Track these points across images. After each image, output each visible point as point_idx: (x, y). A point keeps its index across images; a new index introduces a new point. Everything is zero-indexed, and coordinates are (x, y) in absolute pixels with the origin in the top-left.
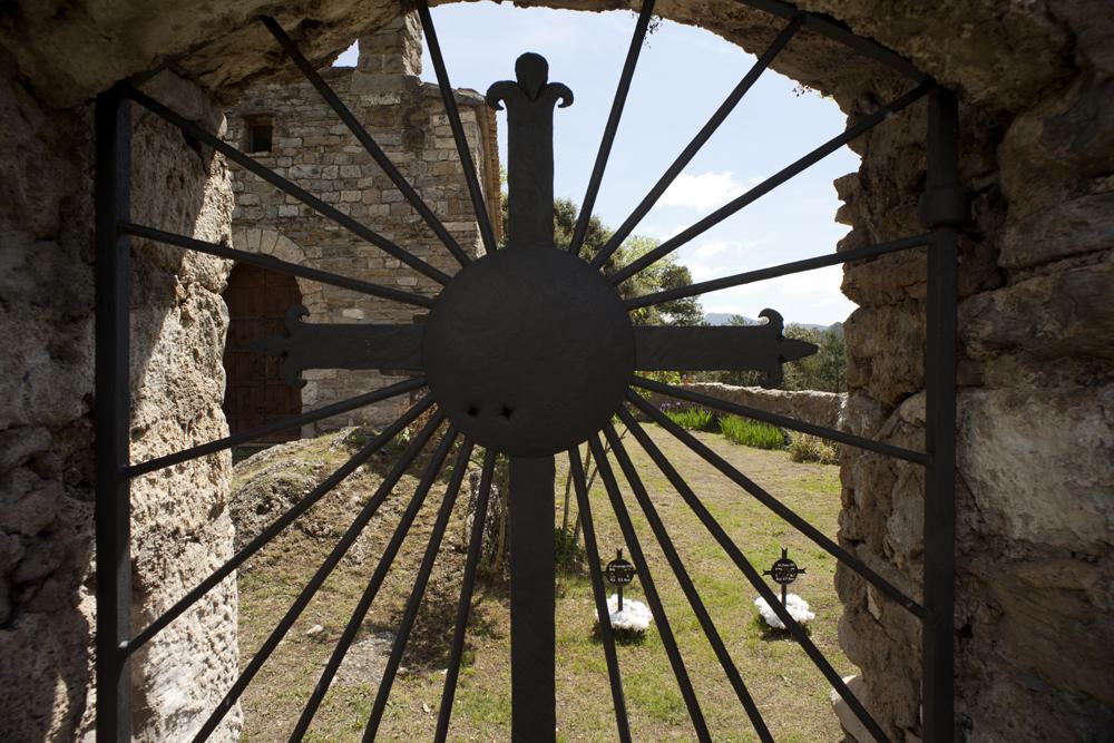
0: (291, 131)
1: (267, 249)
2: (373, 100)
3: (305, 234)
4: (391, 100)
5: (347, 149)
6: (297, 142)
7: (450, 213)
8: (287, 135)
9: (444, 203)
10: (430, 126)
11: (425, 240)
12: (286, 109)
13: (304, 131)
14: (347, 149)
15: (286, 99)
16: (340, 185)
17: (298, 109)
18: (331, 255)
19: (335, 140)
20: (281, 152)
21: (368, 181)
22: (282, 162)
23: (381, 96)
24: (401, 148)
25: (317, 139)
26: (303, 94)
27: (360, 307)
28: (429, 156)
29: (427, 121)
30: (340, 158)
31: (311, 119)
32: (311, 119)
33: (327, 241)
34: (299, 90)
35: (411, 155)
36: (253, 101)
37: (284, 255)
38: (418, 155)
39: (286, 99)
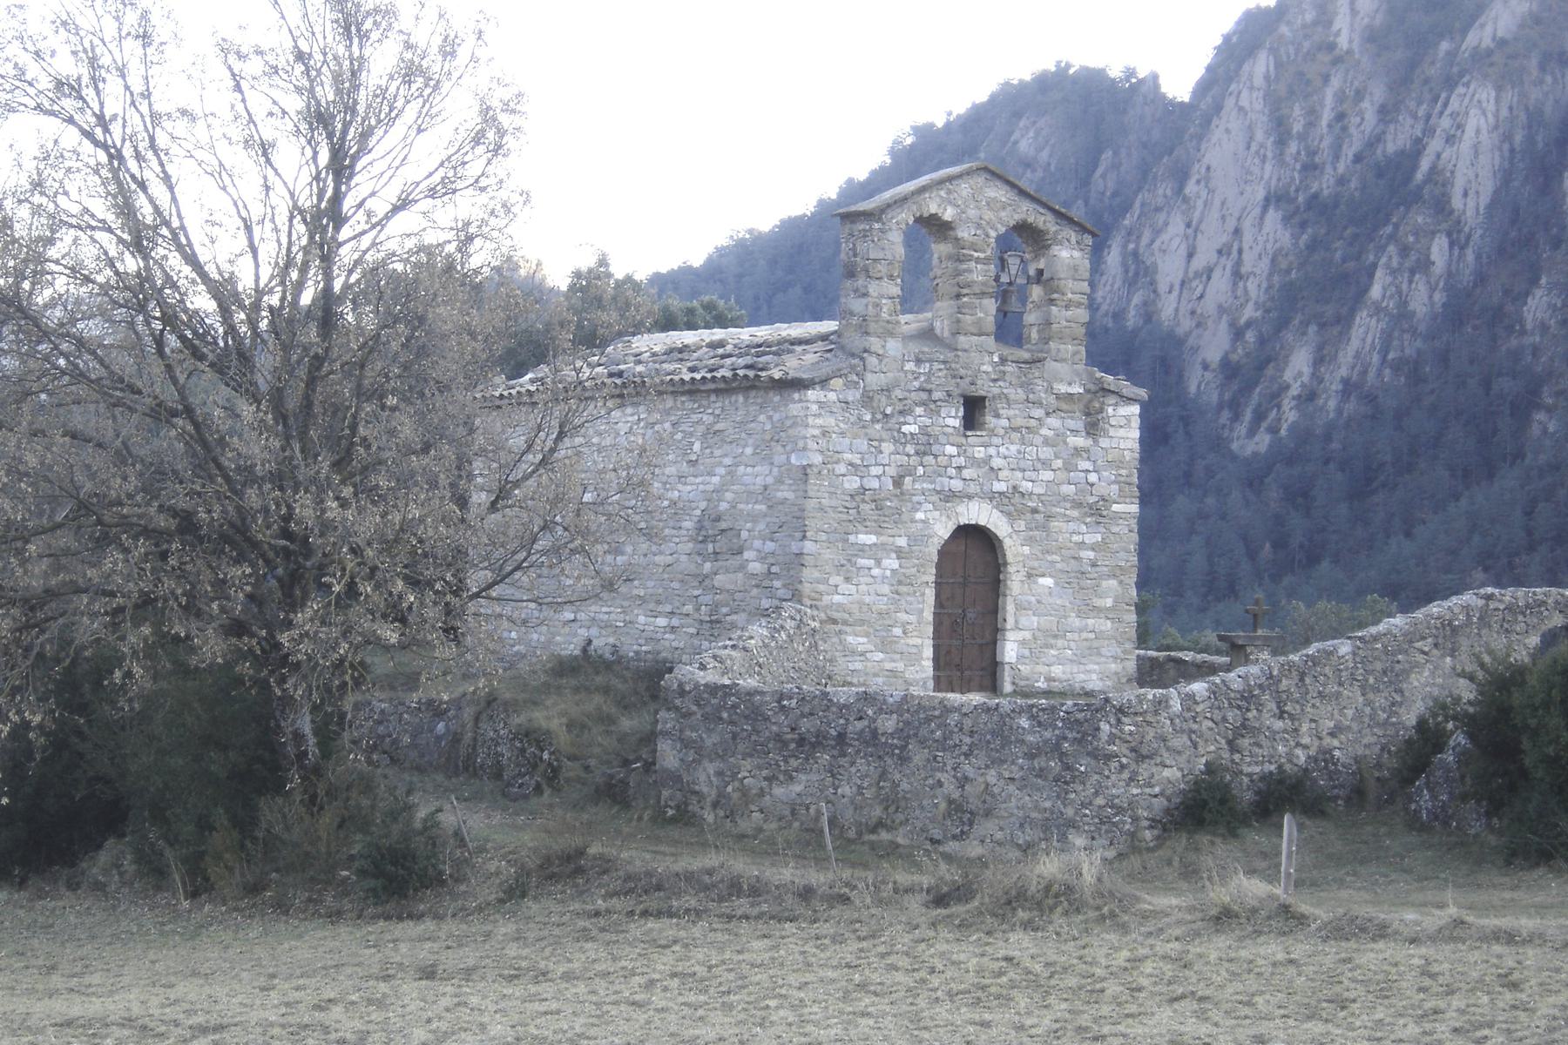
0: (1001, 412)
1: (982, 523)
2: (1063, 388)
3: (1012, 508)
4: (1077, 389)
5: (1044, 431)
6: (1004, 423)
7: (1120, 496)
8: (998, 416)
9: (1116, 487)
10: (1104, 415)
11: (1101, 520)
12: (996, 391)
13: (1011, 412)
14: (1044, 431)
15: (995, 380)
16: (1039, 466)
17: (1005, 391)
18: (1031, 530)
19: (1033, 423)
20: (992, 433)
21: (1059, 463)
22: (996, 440)
23: (1070, 384)
24: (1084, 434)
25: (1019, 422)
26: (1008, 377)
27: (1051, 576)
28: (1104, 442)
29: (1101, 410)
30: (1038, 440)
31: (1016, 402)
32: (1016, 402)
33: (1029, 515)
34: (1004, 373)
35: (1090, 442)
36: (967, 380)
37: (996, 526)
38: (1096, 442)
39: (995, 380)
